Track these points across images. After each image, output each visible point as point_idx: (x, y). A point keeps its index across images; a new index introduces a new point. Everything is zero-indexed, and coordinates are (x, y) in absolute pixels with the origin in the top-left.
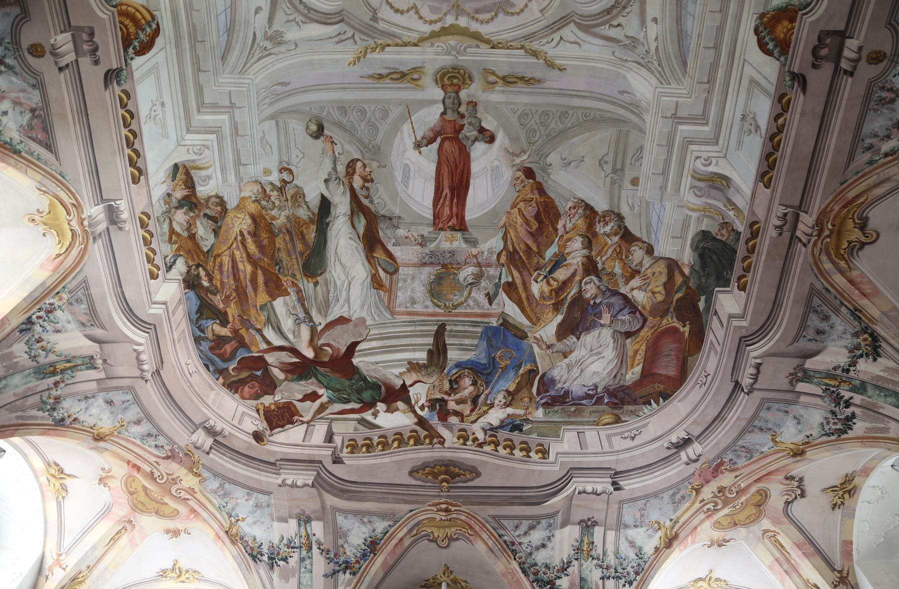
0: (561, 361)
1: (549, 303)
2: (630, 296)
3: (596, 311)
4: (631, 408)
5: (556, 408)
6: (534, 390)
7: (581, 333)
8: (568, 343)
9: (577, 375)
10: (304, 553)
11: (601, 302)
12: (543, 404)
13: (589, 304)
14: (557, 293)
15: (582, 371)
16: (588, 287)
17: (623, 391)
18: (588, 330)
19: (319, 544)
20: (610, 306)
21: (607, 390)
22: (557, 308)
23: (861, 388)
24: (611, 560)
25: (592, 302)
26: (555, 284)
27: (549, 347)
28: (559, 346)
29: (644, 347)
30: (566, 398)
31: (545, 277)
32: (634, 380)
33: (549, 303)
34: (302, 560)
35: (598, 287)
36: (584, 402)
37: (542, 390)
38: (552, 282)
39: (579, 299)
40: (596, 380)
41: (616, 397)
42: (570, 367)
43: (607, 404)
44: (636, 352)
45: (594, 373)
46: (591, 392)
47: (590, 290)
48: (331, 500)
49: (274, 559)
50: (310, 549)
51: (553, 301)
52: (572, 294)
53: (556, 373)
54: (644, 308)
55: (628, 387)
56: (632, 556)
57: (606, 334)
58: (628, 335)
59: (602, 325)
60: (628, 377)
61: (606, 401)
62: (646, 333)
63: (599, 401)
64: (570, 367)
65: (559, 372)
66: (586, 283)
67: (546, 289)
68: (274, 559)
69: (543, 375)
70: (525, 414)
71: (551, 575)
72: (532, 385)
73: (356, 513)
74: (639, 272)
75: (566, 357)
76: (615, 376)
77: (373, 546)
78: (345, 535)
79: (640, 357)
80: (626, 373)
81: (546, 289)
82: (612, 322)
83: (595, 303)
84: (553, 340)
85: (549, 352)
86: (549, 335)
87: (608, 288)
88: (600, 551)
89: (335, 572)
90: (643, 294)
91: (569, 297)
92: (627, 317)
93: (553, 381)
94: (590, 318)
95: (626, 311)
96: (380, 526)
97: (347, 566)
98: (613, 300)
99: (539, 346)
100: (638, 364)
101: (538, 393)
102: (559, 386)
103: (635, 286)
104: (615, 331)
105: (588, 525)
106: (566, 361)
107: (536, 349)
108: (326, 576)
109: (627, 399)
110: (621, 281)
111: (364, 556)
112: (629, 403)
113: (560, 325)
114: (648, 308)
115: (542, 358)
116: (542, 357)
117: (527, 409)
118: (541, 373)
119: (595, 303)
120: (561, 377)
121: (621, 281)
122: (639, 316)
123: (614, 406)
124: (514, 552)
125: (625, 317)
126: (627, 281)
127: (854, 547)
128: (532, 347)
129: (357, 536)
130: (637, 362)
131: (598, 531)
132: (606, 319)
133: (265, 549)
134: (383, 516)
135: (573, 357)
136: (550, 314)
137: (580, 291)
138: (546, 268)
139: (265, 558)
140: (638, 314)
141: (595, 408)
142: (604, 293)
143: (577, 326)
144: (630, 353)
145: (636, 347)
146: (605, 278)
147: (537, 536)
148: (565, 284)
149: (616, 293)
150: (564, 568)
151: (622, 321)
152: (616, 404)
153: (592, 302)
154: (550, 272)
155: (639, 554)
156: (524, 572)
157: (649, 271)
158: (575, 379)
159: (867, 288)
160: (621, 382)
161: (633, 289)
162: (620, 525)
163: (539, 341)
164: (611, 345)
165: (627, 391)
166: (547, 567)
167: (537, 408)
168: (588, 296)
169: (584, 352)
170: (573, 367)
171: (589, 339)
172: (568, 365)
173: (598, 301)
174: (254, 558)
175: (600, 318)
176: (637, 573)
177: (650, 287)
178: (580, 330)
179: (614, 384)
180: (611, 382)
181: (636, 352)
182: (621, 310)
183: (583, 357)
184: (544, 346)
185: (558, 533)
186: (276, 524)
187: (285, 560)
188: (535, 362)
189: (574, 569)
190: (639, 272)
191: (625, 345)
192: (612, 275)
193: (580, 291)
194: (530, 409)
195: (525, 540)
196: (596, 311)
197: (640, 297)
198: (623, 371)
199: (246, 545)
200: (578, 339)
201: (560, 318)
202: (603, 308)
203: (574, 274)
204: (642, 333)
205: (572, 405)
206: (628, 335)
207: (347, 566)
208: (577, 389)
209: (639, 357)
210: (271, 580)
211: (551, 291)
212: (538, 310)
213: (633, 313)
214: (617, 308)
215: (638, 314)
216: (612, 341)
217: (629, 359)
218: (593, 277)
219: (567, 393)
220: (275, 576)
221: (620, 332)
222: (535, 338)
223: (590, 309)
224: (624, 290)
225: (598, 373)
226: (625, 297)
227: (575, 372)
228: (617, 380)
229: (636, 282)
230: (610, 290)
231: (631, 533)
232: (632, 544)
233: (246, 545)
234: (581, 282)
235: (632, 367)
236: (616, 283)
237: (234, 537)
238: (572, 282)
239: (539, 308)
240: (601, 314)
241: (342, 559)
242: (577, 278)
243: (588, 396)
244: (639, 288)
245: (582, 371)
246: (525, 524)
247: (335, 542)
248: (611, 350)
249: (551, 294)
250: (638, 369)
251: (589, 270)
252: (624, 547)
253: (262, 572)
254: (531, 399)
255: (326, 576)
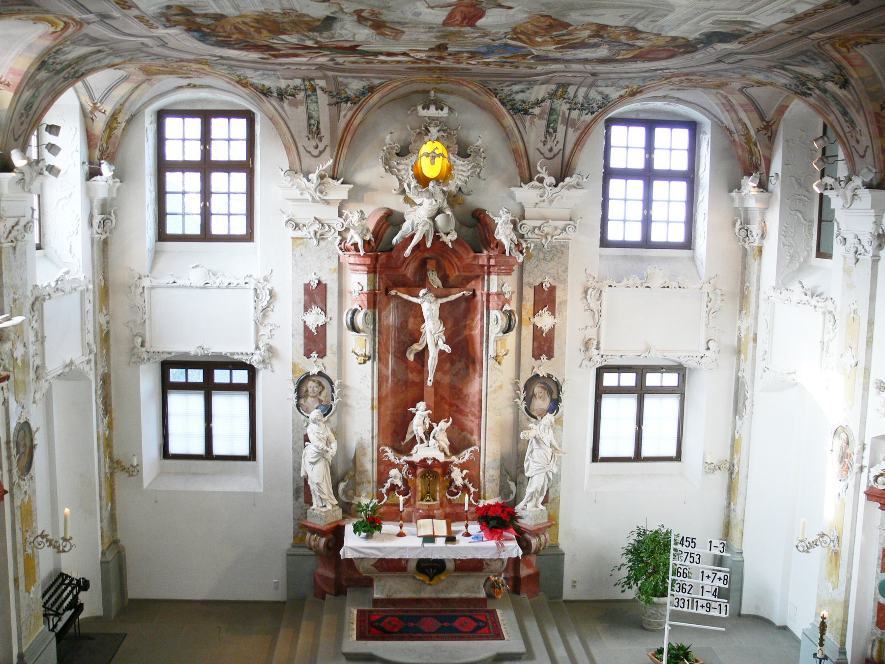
10: (309, 93)
19: (322, 89)
23: (825, 91)
24: (580, 99)
34: (308, 96)
48: (330, 74)
49: (281, 95)
50: (314, 90)
56: (599, 98)
68: (281, 95)
71: (525, 106)
73: (354, 77)
77: (371, 89)
78: (346, 85)
88: (571, 95)
89: (337, 103)
96: (376, 82)
97: (348, 99)
105: (564, 86)
108: (330, 105)
111: (363, 94)
124: (496, 94)
127: (789, 109)
129: (355, 86)
131: (571, 90)
133: (274, 90)
134: (380, 78)
139: (275, 94)
147: (516, 88)
150: (538, 103)
155: (606, 97)
156: (503, 103)
159: (857, 62)
162: (592, 86)
166: (523, 102)
174: (265, 95)
176: (599, 107)
185: (536, 87)
186: (282, 81)
187: (293, 95)
189: (548, 103)
195: (509, 88)
199: (256, 88)
207: (348, 99)
210: (283, 108)
220: (286, 105)
231: (600, 89)
232: (601, 93)
233: (256, 88)
237: (243, 83)
241: (343, 96)
246: (507, 83)
247: (336, 89)
252: (593, 94)
253: (274, 102)
255: (330, 105)
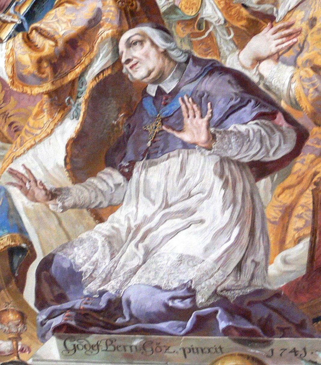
0: (90, 228)
1: (37, 90)
2: (252, 75)
3: (167, 111)
4: (291, 343)
5: (92, 339)
6: (29, 294)
7: (132, 164)
8: (102, 186)
9: (136, 262)
11: (175, 92)
12: (57, 330)
13: (144, 93)
14: (55, 68)
15: (148, 253)
16: (137, 52)
17: (264, 303)
18: (150, 155)
20: (201, 100)
21: (220, 298)
22: (60, 101)
25: (152, 90)
26: (48, 48)
27: (52, 195)
28: (80, 193)
29: (307, 199)
30: (114, 316)
31: (19, 28)
32: (292, 277)
33: (37, 90)
35: (165, 53)
36: (163, 326)
37: (48, 296)
38: (38, 40)
39: (114, 83)
40: (189, 274)
41: (247, 316)
42: (114, 244)
43: (226, 332)
44: (288, 211)
45: (181, 259)
46: (178, 304)
47: (144, 57)
51: (48, 87)
52: (96, 68)
53: (79, 257)
54: (296, 105)
55: (277, 294)
57: (202, 168)
58: (261, 169)
59: (186, 145)
60: (272, 270)
61: (222, 325)
62: (306, 164)
63: (204, 324)
64: (114, 244)
65: (88, 253)
66: (130, 44)
67: (27, 58)
69: (47, 263)
70: (15, 351)
72: (21, 284)
74: (271, 18)
75: (100, 219)
76: (239, 267)
79: (301, 221)
80: (268, 262)
81: (27, 58)
82: (212, 137)
83: (160, 91)
84: (62, 179)
85: (54, 206)
86: (50, 166)
87: (191, 58)
90: (287, 72)
91: (89, 77)
92: (253, 126)
93: (75, 277)
94: (152, 128)
95: (248, 111)
98: (208, 84)
99: (26, 193)
100: (298, 241)
101: (41, 303)
102: (93, 287)
103: (264, 53)
104: (223, 160)
106: (104, 228)
107: (20, 200)
109: (277, 322)
110: (224, 41)
112: (284, 333)
113: (76, 144)
114: (306, 105)
115: (38, 220)
116: (39, 219)
117: (18, 337)
118: (40, 257)
119: (160, 91)
120: (96, 264)
121: (224, 41)
122: (285, 125)
123: (246, 337)
125: (245, 124)
126: (242, 39)
128: (7, 195)
130: (292, 234)
132: (195, 129)
135: (119, 219)
136: (45, 118)
137: (117, 62)
138: (19, 7)
140: (280, 119)
141: (195, 340)
142: (181, 67)
143: (120, 147)
144: (272, 213)
145: (286, 199)
146: (179, 31)
148: (74, 46)
149: (215, 69)
151: (239, 134)
152: (251, 333)
153: (152, 90)
154: (31, 16)
157: (299, 15)
158: (134, 272)
160: (258, 283)
161: (258, 60)
163: (24, 181)
164: (218, 193)
165: (275, 303)
167: (43, 338)
168: (139, 74)
169: (145, 209)
170: (122, 243)
171: (156, 176)
172: (110, 240)
173: (168, 86)
175: (180, 127)
177: (305, 55)
178: (130, 154)
179: (238, 287)
180: (230, 282)
181: (288, 211)
182: (233, 110)
183: (147, 220)
184: (40, 194)
188: (22, 230)
190: (271, 18)
191: (254, 193)
192: (198, 24)
193: (117, 62)
194: (25, 341)
196: (167, 111)
197: (282, 79)
198: (260, 255)
200: (128, 176)
201: (70, 127)
202: (185, 104)
203: (95, 22)
204: (299, 166)
205: (134, 332)
206: (261, 169)
208: (140, 292)
209: (296, 223)
211: (40, 61)
212: (10, 107)
213: (272, 116)
214: (222, 105)
215: (280, 119)
216: (219, 183)
217: (269, 227)
218: (148, 30)
219: (115, 305)
221: (238, 163)
222: (12, 172)
223: (148, 104)
224: (236, 60)
225: (192, 258)
226: (240, 79)
227: (131, 255)
228: (245, 278)
229: (265, 41)
230: (197, 61)
234: (115, 40)
235: (282, 245)
236: (211, 44)
238: (92, 42)
239: (13, 100)
240: (180, 117)
242: (106, 31)
243: (171, 313)
244: (277, 57)
245: (148, 253)
248: (219, 204)
249: (39, 68)
250: (298, 253)
251: (133, 13)
254: (23, 317)
